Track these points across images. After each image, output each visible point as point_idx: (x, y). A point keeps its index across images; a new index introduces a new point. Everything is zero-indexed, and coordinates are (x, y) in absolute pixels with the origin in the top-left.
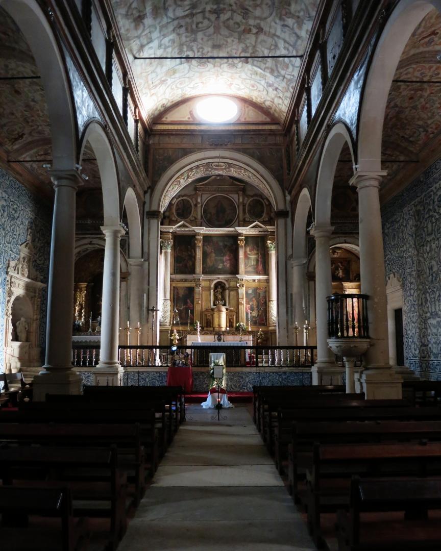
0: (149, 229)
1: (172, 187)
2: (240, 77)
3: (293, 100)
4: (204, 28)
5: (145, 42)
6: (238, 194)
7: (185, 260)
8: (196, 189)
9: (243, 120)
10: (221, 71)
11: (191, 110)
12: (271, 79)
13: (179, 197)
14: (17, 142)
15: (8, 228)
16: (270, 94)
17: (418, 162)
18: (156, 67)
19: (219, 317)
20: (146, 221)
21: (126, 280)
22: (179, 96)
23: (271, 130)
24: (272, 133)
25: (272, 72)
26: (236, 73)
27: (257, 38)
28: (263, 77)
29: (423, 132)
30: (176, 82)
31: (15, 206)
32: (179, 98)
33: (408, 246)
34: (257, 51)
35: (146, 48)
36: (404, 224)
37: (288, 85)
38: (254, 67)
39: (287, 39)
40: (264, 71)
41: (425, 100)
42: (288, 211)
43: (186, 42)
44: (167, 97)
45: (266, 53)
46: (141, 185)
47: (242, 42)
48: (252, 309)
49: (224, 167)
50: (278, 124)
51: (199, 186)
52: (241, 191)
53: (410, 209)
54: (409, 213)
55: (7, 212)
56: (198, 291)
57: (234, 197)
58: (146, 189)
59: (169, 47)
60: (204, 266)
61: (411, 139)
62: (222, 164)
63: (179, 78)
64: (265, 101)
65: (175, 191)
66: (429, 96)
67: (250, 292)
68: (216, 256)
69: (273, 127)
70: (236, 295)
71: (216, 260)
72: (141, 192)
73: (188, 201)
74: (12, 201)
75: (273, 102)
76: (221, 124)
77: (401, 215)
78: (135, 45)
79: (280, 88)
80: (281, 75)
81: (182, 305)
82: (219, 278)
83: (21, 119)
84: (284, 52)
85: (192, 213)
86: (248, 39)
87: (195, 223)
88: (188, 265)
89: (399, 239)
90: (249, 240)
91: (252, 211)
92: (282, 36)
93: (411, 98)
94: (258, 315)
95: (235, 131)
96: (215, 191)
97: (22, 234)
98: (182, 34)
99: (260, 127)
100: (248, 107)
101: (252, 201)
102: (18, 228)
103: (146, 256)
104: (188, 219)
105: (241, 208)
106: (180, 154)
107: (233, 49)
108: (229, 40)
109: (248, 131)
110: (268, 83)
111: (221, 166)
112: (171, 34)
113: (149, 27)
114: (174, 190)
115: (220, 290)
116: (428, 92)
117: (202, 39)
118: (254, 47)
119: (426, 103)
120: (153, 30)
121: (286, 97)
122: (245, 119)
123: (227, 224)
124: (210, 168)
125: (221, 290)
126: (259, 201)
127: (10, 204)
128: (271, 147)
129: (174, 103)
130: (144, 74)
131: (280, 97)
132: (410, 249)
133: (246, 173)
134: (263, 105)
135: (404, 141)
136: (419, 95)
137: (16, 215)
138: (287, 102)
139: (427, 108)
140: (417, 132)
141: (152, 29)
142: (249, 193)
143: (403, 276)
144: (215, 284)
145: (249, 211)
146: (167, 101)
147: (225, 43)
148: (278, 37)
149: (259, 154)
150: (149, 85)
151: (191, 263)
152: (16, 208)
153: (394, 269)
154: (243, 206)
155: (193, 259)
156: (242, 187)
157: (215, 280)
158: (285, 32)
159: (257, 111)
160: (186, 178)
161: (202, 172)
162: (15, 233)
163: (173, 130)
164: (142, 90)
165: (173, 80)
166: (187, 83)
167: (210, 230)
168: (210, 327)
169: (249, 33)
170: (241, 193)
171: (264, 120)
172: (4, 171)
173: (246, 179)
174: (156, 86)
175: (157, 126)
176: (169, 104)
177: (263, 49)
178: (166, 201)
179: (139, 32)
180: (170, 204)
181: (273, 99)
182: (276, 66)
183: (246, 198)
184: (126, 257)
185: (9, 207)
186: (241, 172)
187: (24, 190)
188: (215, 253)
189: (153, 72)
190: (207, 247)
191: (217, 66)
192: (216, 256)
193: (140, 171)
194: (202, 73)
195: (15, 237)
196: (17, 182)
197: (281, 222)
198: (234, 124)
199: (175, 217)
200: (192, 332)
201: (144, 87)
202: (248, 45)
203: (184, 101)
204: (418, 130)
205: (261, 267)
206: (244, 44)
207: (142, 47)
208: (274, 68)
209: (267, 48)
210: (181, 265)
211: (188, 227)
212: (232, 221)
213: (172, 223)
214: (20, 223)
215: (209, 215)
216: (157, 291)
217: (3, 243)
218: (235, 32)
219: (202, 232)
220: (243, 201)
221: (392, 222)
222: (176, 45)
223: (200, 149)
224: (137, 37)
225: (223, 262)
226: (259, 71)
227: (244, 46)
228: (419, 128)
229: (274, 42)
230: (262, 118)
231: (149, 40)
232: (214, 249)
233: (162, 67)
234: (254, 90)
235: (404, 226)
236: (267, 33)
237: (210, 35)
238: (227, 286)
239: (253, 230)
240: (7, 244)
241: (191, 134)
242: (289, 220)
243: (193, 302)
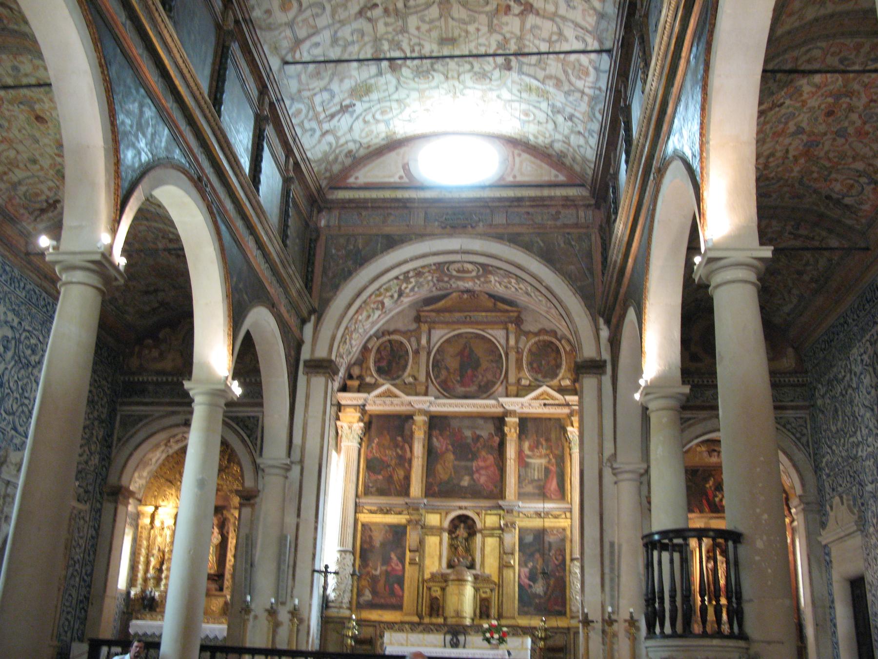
0: (308, 397)
1: (365, 314)
2: (498, 97)
3: (604, 135)
4: (418, 9)
5: (302, 33)
6: (507, 329)
7: (389, 466)
8: (418, 319)
9: (510, 179)
10: (461, 87)
11: (405, 161)
12: (559, 99)
13: (383, 334)
14: (45, 217)
15: (11, 384)
16: (560, 129)
17: (867, 249)
18: (331, 80)
19: (461, 594)
20: (302, 379)
21: (252, 501)
22: (383, 135)
23: (566, 198)
24: (568, 202)
25: (558, 84)
26: (491, 90)
27: (523, 23)
28: (543, 94)
29: (869, 184)
30: (373, 110)
31: (33, 341)
32: (383, 139)
33: (865, 432)
34: (525, 46)
35: (305, 46)
36: (854, 385)
37: (593, 109)
38: (523, 77)
39: (579, 20)
40: (543, 83)
41: (860, 117)
42: (605, 361)
43: (387, 33)
44: (357, 138)
45: (544, 47)
46: (293, 306)
47: (495, 31)
48: (532, 577)
49: (474, 274)
50: (582, 185)
51: (427, 314)
52: (512, 322)
53: (862, 351)
54: (862, 361)
55: (13, 350)
56: (412, 537)
57: (497, 335)
58: (305, 313)
59: (353, 42)
60: (431, 480)
61: (847, 201)
62: (470, 267)
63: (379, 101)
64: (553, 142)
65: (373, 324)
66: (866, 107)
67: (529, 539)
68: (456, 460)
69: (572, 192)
70: (497, 545)
71: (454, 467)
72: (293, 321)
73: (401, 343)
74: (28, 331)
75: (569, 144)
76: (461, 189)
77: (846, 365)
78: (285, 38)
79: (577, 114)
80: (579, 91)
81: (379, 564)
82: (460, 508)
83: (51, 172)
84: (579, 46)
85: (409, 367)
86: (507, 24)
87: (410, 389)
88: (395, 477)
89: (847, 418)
90: (529, 424)
91: (535, 365)
92: (571, 15)
93: (830, 113)
94: (545, 593)
95: (493, 200)
96: (458, 322)
98: (377, 20)
99: (546, 192)
100: (519, 155)
101: (536, 343)
103: (296, 455)
104: (397, 381)
105: (513, 356)
106: (379, 247)
107: (480, 45)
108: (471, 28)
109: (519, 200)
110: (553, 106)
111: (468, 272)
112: (356, 19)
113: (310, 6)
114: (371, 320)
115: (462, 532)
116: (864, 100)
117: (418, 28)
118: (520, 39)
119: (865, 123)
120: (319, 11)
121: (591, 132)
122: (515, 177)
123: (484, 391)
124: (446, 275)
125: (465, 535)
126: (552, 343)
128: (568, 230)
129: (371, 149)
130: (306, 94)
131: (579, 133)
132: (870, 440)
133: (521, 286)
134: (550, 151)
135: (831, 205)
136: (844, 106)
138: (593, 141)
139: (867, 133)
140: (856, 185)
141: (315, 10)
142: (529, 326)
143: (859, 502)
144: (453, 521)
145: (530, 364)
146: (358, 145)
147: (463, 34)
148: (564, 19)
149: (542, 244)
150: (316, 116)
151: (401, 473)
152: (36, 345)
153: (841, 486)
154: (518, 352)
155: (406, 465)
156: (515, 314)
157: (454, 510)
158: (574, 8)
159: (538, 162)
160: (396, 296)
161: (431, 284)
162: (26, 395)
163: (366, 201)
164: (301, 124)
165: (366, 106)
166: (395, 112)
167: (444, 405)
168: (438, 615)
169: (506, 14)
170: (512, 327)
171: (553, 179)
172: (16, 271)
173: (522, 299)
174: (332, 116)
175: (336, 192)
176: (362, 152)
177: (537, 42)
178: (353, 342)
179: (291, 14)
180: (365, 349)
181: (568, 138)
182: (565, 72)
183: (523, 338)
184: (256, 455)
185: (18, 341)
186: (510, 283)
188: (454, 453)
189: (325, 89)
190: (437, 439)
191: (453, 78)
192: (456, 460)
193: (290, 276)
194: (424, 90)
195: (26, 402)
196: (44, 294)
197: (589, 383)
198: (492, 187)
199: (372, 376)
200: (397, 626)
201: (307, 116)
202: (508, 36)
203: (393, 145)
204: (858, 182)
205: (553, 485)
206: (502, 34)
207: (298, 42)
208: (563, 77)
209: (544, 40)
210: (380, 477)
211: (396, 396)
212: (494, 384)
213: (364, 387)
215: (444, 373)
216: (316, 529)
218: (480, 13)
219: (425, 407)
220: (517, 342)
221: (830, 382)
222: (366, 39)
223: (421, 236)
224: (285, 24)
225: (471, 474)
226: (535, 83)
227: (500, 38)
228: (860, 176)
229: (555, 29)
230: (548, 174)
231: (311, 31)
232: (453, 446)
233: (341, 81)
234: (529, 122)
235: (853, 389)
236: (541, 12)
237: (432, 21)
238: (479, 525)
239: (536, 403)
241: (404, 205)
242: (607, 379)
243: (402, 559)
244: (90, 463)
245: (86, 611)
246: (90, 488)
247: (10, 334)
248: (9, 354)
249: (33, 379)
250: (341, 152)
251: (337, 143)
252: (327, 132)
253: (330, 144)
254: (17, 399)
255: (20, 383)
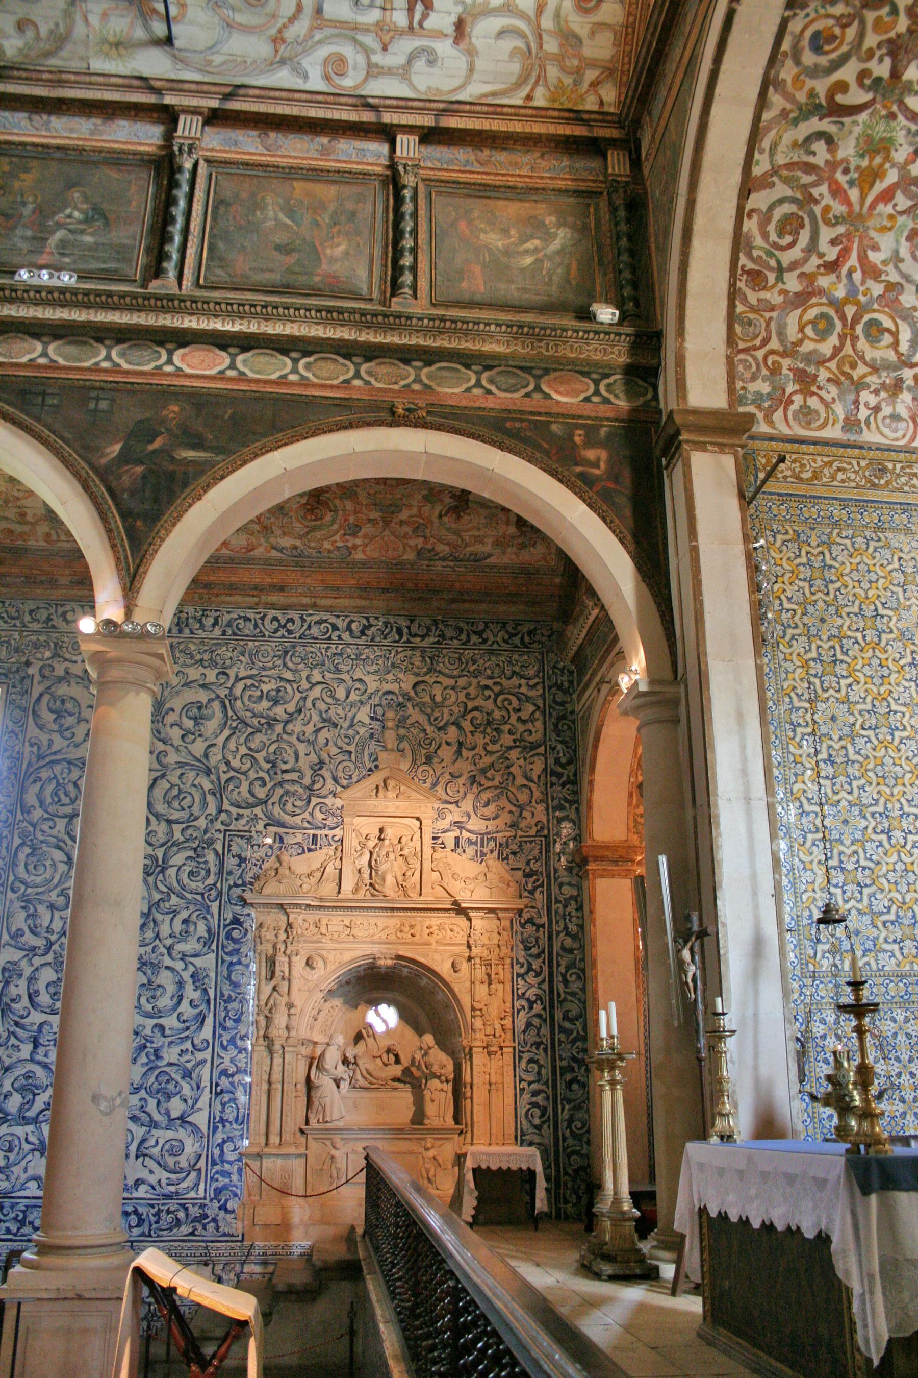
15: (235, 763)
31: (265, 688)
55: (219, 715)
97: (341, 757)
102: (302, 748)
127: (238, 691)
137: (279, 711)
187: (319, 623)
195: (294, 776)
196: (272, 613)
201: (367, 52)
214: (310, 729)
217: (212, 809)
240: (234, 811)
244: (523, 825)
245: (583, 1085)
246: (534, 866)
247: (203, 696)
248: (211, 726)
249: (294, 739)
250: (557, 15)
251: (522, 15)
252: (460, 25)
253: (502, 33)
254: (261, 779)
255: (260, 757)
